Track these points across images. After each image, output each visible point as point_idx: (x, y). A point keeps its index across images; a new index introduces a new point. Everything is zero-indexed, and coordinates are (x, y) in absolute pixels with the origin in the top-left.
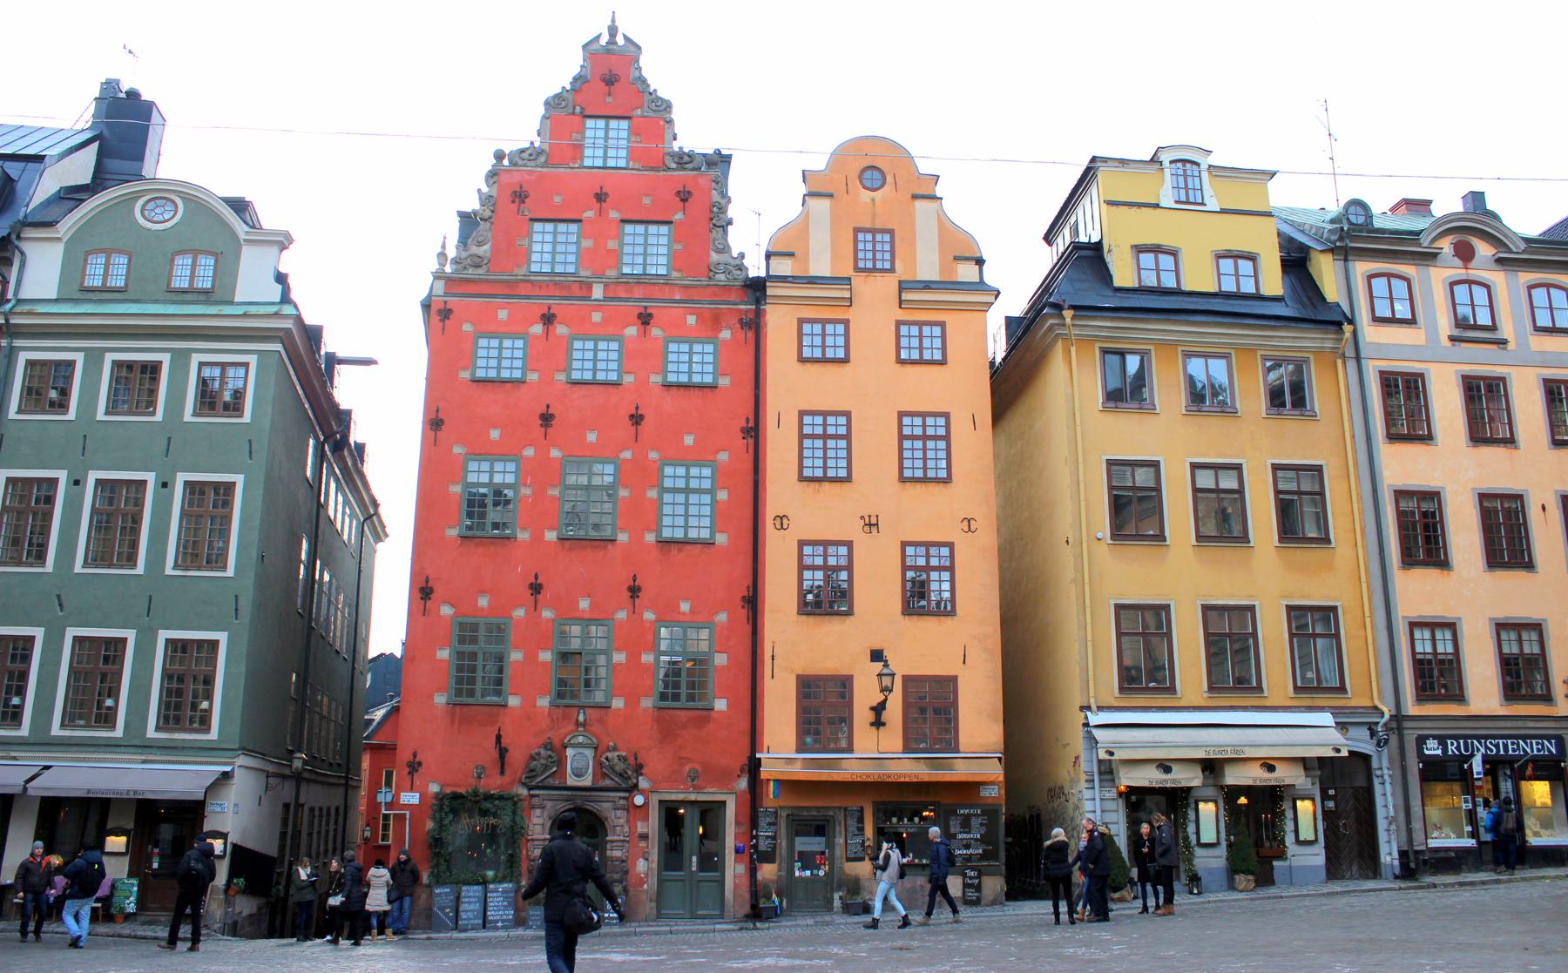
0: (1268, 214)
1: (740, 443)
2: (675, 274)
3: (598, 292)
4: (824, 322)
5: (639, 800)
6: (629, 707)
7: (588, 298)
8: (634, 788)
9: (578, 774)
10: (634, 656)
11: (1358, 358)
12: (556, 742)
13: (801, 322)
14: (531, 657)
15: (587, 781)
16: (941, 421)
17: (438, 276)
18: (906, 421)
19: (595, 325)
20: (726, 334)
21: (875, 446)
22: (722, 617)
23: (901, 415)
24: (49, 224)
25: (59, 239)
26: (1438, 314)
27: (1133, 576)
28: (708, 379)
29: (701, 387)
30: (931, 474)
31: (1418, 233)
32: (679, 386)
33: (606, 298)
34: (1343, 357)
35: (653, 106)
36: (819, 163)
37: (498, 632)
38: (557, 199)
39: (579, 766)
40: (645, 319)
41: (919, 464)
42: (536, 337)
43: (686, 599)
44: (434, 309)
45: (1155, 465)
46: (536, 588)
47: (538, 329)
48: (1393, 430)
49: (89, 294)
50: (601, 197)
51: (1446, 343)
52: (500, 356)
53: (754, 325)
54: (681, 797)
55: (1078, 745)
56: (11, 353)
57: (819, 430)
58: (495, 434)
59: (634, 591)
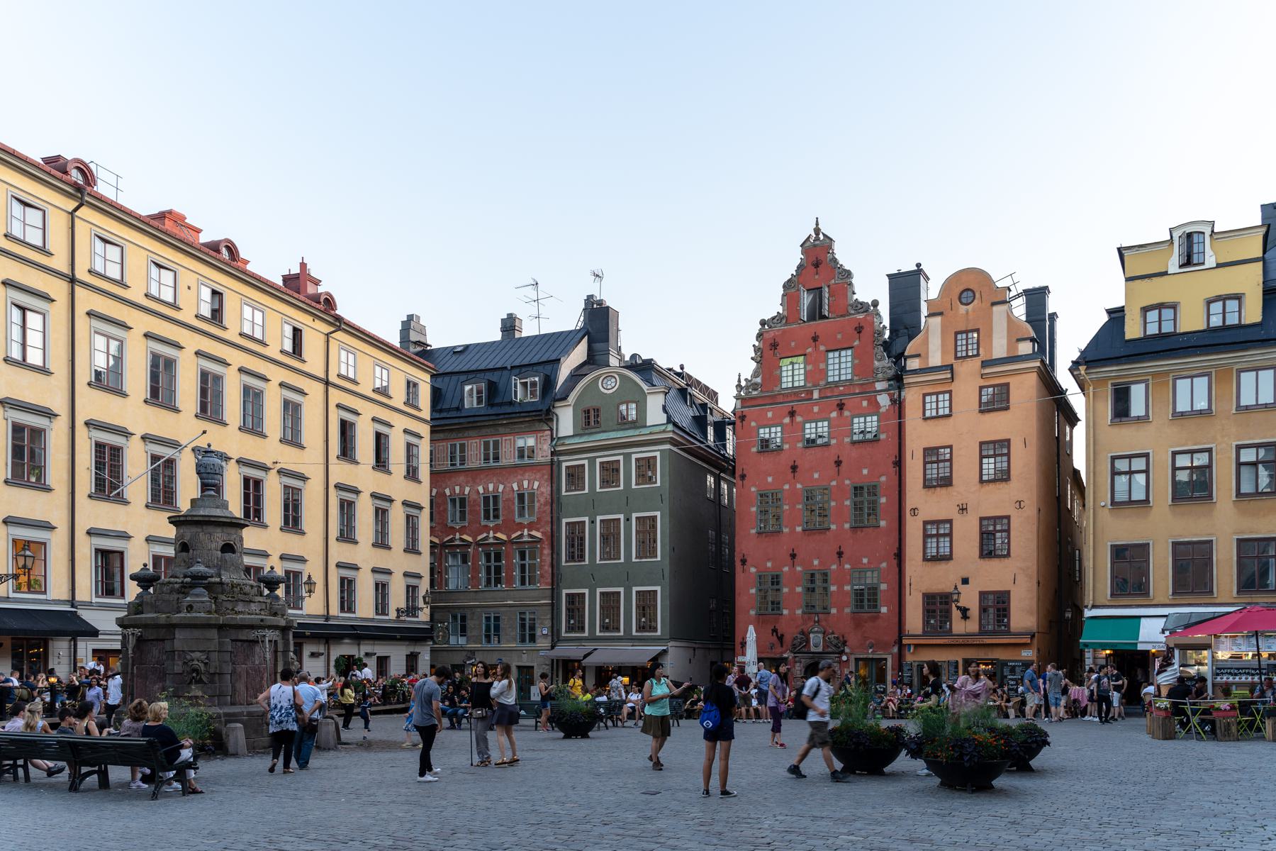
3: (816, 395)
4: (937, 394)
40: (841, 406)
45: (1147, 455)
47: (787, 420)
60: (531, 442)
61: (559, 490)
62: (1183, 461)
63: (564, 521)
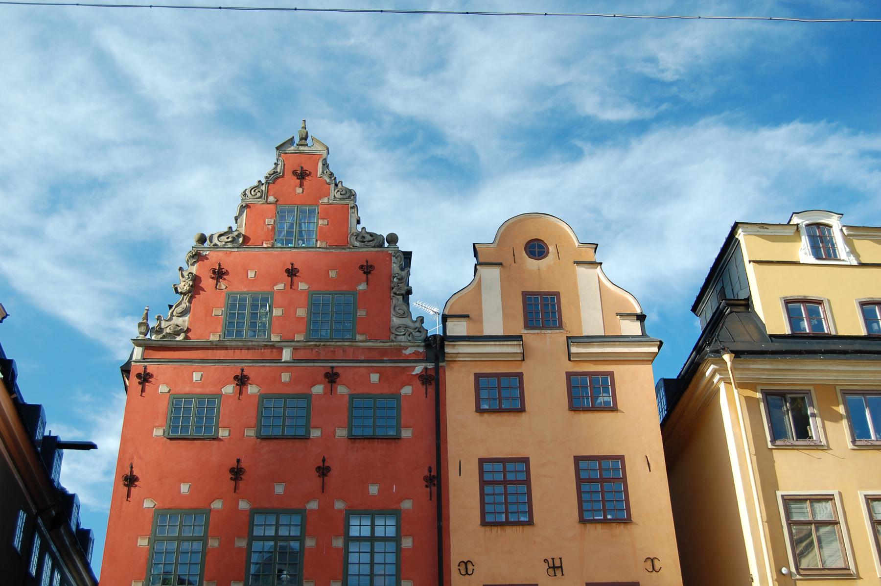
3: (286, 355)
7: (279, 360)
13: (477, 376)
19: (285, 384)
20: (407, 390)
23: (578, 459)
33: (295, 361)
35: (338, 195)
36: (488, 237)
38: (251, 274)
40: (332, 378)
42: (228, 396)
50: (292, 272)
53: (433, 382)
57: (500, 477)
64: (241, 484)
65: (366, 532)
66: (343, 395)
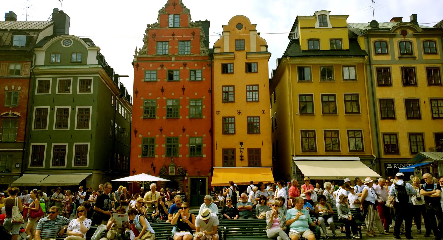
0: (346, 27)
1: (208, 94)
2: (192, 54)
3: (173, 59)
5: (186, 178)
6: (183, 156)
7: (171, 60)
8: (185, 176)
9: (172, 172)
10: (184, 145)
11: (370, 65)
12: (166, 165)
14: (160, 146)
15: (174, 174)
16: (257, 87)
17: (135, 56)
18: (248, 87)
19: (174, 67)
20: (204, 68)
21: (240, 94)
22: (204, 135)
23: (247, 86)
24: (41, 47)
25: (44, 51)
26: (395, 51)
27: (305, 124)
28: (200, 79)
29: (199, 81)
30: (254, 100)
31: (389, 29)
32: (193, 81)
33: (175, 60)
34: (366, 65)
37: (153, 141)
39: (172, 171)
40: (185, 65)
41: (251, 97)
42: (159, 70)
43: (196, 131)
44: (135, 65)
46: (161, 130)
47: (159, 69)
48: (380, 83)
49: (52, 64)
51: (397, 58)
52: (151, 76)
53: (211, 65)
54: (196, 177)
55: (292, 165)
56: (35, 79)
58: (150, 94)
59: (184, 130)
60: (18, 67)
61: (34, 92)
62: (325, 99)
63: (35, 108)
64: (163, 93)
65: (194, 104)
66: (188, 70)
